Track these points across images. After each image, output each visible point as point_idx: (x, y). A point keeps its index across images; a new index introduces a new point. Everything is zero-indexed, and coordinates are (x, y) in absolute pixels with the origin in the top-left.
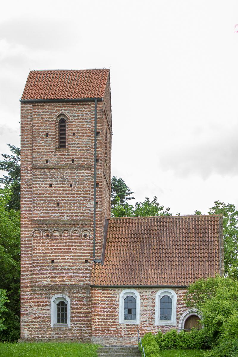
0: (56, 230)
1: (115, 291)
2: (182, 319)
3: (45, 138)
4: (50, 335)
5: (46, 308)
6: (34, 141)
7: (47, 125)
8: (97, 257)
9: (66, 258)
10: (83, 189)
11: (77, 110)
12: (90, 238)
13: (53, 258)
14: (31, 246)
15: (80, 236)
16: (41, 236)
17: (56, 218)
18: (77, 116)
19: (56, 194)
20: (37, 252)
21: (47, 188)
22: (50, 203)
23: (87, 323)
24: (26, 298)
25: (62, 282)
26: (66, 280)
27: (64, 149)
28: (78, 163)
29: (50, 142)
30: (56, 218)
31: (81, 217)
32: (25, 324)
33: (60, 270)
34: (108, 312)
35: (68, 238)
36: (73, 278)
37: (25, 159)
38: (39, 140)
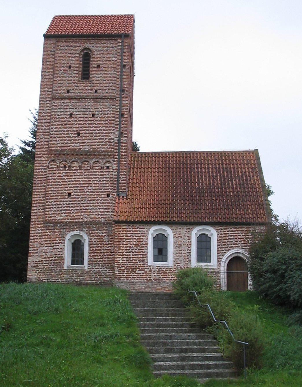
0: (75, 161)
1: (143, 227)
2: (224, 261)
3: (67, 70)
4: (63, 278)
5: (59, 247)
6: (55, 72)
7: (70, 58)
8: (121, 190)
9: (85, 191)
10: (106, 119)
11: (103, 44)
12: (113, 169)
13: (69, 191)
14: (45, 178)
15: (102, 168)
16: (57, 167)
17: (75, 148)
18: (102, 50)
19: (76, 123)
20: (52, 184)
21: (67, 117)
22: (69, 133)
23: (107, 265)
24: (36, 235)
25: (79, 217)
26: (84, 216)
27: (87, 80)
28: (101, 94)
29: (73, 73)
30: (75, 148)
31: (104, 147)
32: (33, 265)
33: (77, 204)
34: (135, 252)
35: (89, 169)
36: (92, 213)
37: (45, 89)
38: (61, 72)
